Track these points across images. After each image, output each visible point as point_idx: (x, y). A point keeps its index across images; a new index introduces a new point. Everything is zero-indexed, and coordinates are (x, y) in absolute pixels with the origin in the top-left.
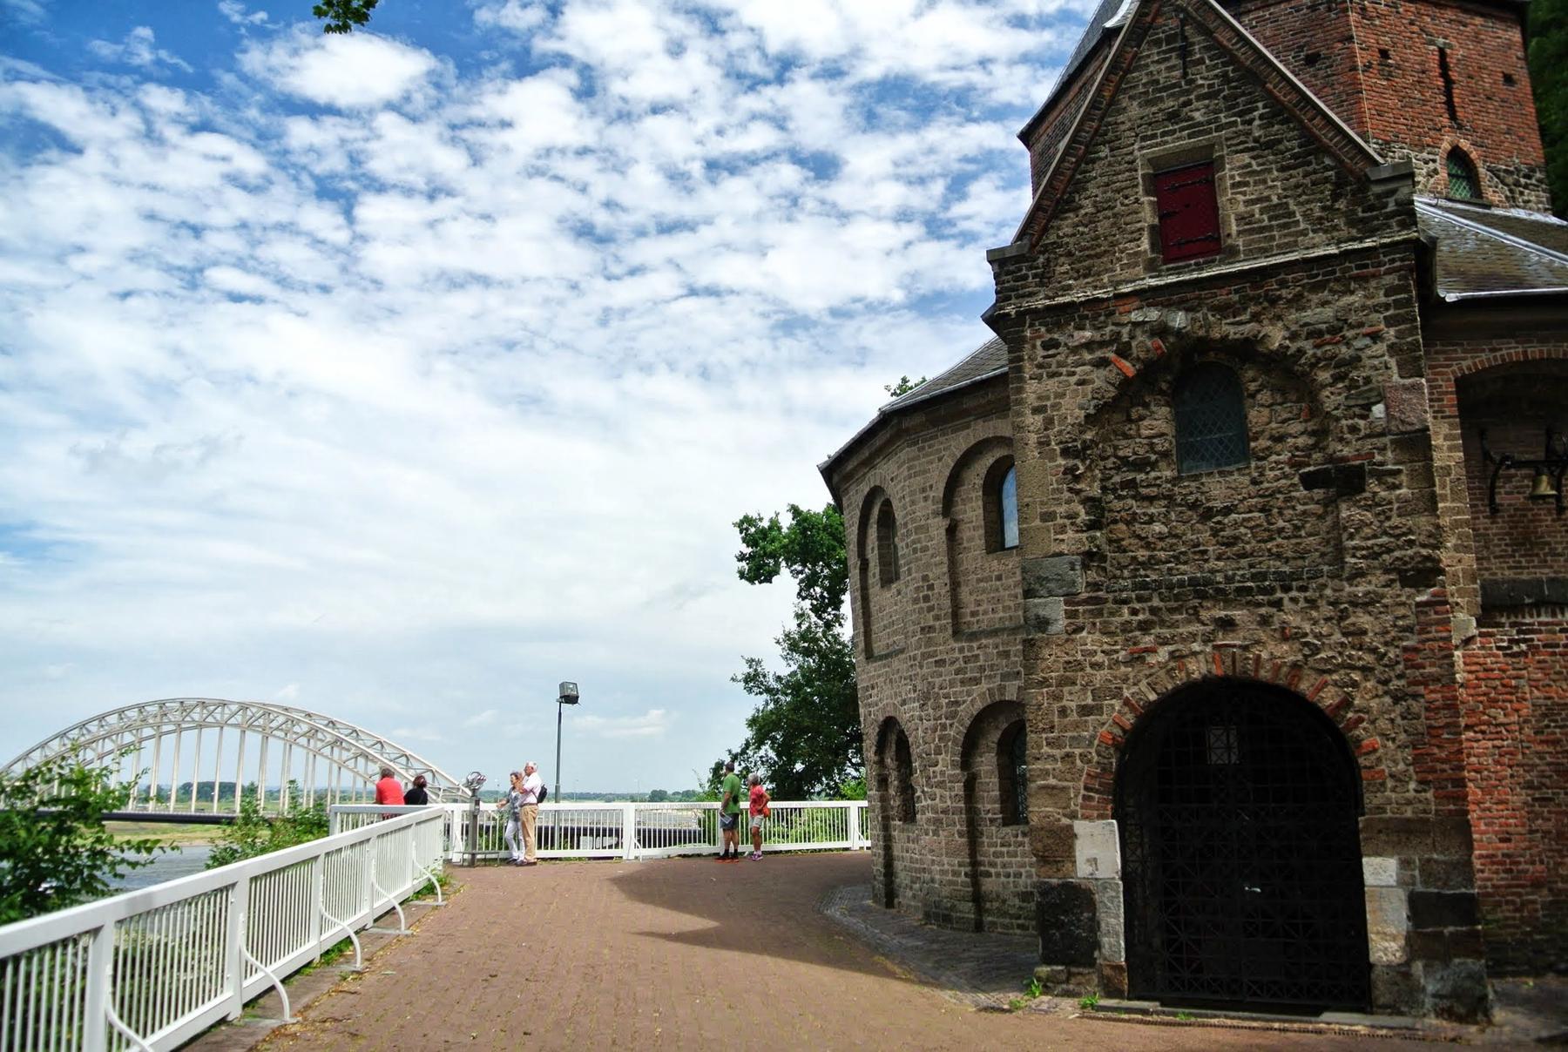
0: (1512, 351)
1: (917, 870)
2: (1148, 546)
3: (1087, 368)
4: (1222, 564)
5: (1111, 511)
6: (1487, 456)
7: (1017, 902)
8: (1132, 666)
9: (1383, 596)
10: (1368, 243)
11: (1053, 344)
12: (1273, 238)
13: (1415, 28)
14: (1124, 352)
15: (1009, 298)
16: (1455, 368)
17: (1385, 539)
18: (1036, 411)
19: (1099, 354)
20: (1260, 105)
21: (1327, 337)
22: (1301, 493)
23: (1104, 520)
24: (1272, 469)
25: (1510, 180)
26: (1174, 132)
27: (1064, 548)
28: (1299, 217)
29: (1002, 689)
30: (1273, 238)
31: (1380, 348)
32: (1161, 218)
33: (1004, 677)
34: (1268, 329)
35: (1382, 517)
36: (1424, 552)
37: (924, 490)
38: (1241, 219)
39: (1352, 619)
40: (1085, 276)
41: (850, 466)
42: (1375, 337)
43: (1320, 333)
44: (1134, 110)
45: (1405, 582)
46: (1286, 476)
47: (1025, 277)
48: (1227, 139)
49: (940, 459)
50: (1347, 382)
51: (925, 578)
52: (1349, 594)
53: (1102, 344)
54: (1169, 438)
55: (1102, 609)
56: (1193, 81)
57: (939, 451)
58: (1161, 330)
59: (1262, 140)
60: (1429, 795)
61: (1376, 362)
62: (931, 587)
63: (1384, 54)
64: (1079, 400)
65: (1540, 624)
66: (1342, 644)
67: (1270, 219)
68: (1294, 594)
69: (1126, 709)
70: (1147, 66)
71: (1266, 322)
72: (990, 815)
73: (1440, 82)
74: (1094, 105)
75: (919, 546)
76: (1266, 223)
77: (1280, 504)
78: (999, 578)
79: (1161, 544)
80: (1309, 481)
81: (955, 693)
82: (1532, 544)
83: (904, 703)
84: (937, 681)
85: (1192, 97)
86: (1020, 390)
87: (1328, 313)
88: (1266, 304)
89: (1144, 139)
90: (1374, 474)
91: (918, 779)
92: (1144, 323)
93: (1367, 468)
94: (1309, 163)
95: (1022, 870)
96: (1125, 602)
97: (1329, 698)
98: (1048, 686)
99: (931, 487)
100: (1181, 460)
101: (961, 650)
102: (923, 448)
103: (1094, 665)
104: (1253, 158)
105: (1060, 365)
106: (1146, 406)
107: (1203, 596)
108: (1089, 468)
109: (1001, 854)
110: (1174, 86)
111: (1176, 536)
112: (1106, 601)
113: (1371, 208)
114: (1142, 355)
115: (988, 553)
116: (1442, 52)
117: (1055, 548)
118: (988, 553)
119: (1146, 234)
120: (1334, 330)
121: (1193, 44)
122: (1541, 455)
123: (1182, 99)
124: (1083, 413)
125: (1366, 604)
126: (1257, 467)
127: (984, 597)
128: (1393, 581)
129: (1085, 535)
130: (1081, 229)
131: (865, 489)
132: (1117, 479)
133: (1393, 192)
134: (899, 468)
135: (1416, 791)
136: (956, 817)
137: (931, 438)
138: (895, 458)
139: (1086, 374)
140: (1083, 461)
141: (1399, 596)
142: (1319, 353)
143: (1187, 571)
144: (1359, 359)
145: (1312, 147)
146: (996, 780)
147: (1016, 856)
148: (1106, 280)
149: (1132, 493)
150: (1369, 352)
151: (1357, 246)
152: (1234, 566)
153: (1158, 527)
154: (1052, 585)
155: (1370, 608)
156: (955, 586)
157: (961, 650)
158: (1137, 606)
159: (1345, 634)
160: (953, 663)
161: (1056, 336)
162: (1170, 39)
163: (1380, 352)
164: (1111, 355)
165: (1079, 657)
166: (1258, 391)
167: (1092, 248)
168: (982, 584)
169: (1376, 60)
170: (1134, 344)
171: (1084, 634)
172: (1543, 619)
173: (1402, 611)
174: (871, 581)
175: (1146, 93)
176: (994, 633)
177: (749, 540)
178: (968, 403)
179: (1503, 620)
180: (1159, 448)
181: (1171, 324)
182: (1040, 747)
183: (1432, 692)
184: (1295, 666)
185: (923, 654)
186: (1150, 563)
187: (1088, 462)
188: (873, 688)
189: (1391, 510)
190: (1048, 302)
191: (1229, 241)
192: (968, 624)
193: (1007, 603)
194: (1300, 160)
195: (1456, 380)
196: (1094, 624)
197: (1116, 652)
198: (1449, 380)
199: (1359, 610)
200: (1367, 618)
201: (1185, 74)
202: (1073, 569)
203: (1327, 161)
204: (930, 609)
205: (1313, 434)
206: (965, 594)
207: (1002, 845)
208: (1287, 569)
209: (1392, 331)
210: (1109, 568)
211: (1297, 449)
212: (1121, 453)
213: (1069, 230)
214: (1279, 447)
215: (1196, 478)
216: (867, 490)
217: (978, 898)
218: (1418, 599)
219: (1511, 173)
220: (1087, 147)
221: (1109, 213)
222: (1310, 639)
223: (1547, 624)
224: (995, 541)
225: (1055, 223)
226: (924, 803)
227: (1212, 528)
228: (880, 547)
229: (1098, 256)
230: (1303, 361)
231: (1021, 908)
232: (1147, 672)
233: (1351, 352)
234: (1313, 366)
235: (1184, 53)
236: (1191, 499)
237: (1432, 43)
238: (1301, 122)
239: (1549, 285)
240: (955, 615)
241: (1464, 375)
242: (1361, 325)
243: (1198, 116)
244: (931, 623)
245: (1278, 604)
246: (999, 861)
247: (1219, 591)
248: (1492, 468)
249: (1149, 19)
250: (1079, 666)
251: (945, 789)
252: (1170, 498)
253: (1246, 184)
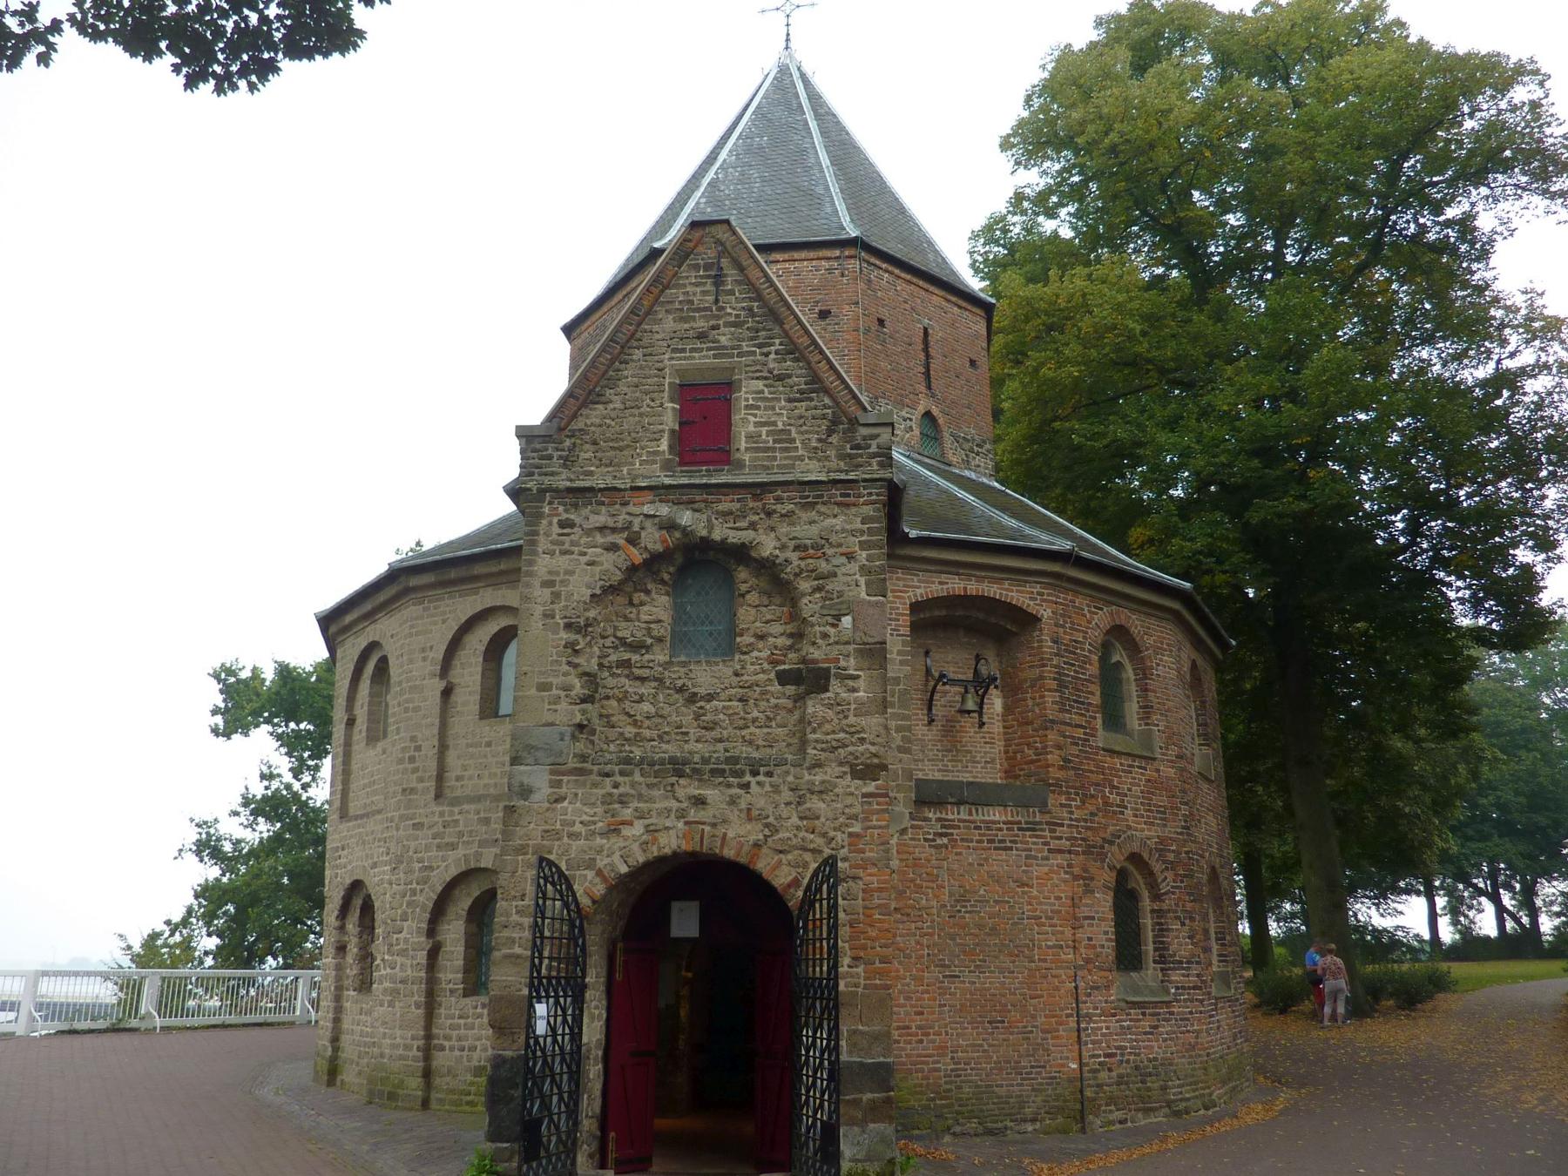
0: (955, 585)
1: (365, 1044)
2: (635, 723)
3: (598, 550)
4: (700, 746)
5: (605, 687)
6: (928, 672)
7: (469, 1078)
8: (608, 839)
9: (835, 786)
10: (851, 476)
11: (571, 525)
12: (775, 458)
14: (633, 541)
15: (532, 474)
16: (911, 594)
17: (842, 735)
18: (548, 584)
19: (611, 538)
20: (777, 341)
21: (811, 551)
22: (776, 688)
23: (597, 696)
24: (752, 664)
25: (967, 446)
26: (701, 350)
27: (558, 718)
28: (798, 444)
29: (478, 856)
30: (775, 458)
31: (853, 567)
32: (681, 424)
33: (482, 844)
34: (762, 538)
35: (841, 716)
36: (873, 749)
37: (423, 650)
38: (749, 437)
39: (808, 805)
40: (606, 466)
41: (348, 619)
42: (850, 557)
43: (805, 548)
44: (669, 323)
45: (857, 774)
46: (764, 672)
47: (550, 457)
48: (747, 366)
49: (444, 621)
50: (823, 594)
51: (413, 739)
52: (808, 782)
53: (614, 530)
54: (665, 624)
55: (585, 781)
56: (723, 308)
57: (444, 613)
58: (670, 526)
59: (775, 372)
60: (860, 969)
61: (849, 578)
62: (418, 748)
63: (881, 322)
64: (587, 579)
65: (959, 820)
66: (798, 828)
67: (775, 441)
68: (761, 778)
69: (598, 880)
70: (684, 286)
71: (761, 531)
72: (451, 986)
73: (922, 356)
74: (633, 311)
75: (411, 705)
76: (771, 444)
77: (756, 696)
78: (489, 744)
79: (647, 723)
80: (783, 678)
81: (429, 858)
82: (957, 751)
83: (375, 865)
84: (413, 844)
85: (721, 322)
86: (531, 563)
87: (814, 530)
88: (762, 516)
89: (675, 350)
90: (837, 676)
91: (379, 947)
92: (654, 516)
93: (833, 671)
94: (811, 400)
95: (478, 1043)
96: (607, 775)
98: (524, 854)
99: (431, 648)
100: (673, 646)
101: (442, 814)
102: (429, 608)
103: (570, 835)
104: (766, 386)
105: (573, 543)
106: (648, 592)
107: (680, 774)
108: (589, 644)
109: (458, 1027)
110: (705, 309)
111: (661, 716)
112: (590, 772)
113: (857, 447)
114: (650, 546)
115: (481, 719)
116: (926, 330)
117: (549, 718)
118: (481, 719)
119: (666, 435)
120: (816, 547)
121: (726, 275)
122: (970, 676)
123: (711, 323)
124: (589, 592)
125: (821, 792)
126: (740, 661)
127: (471, 762)
128: (845, 773)
129: (578, 707)
130: (608, 421)
131: (362, 643)
132: (613, 658)
133: (877, 436)
134: (401, 625)
135: (849, 966)
136: (415, 987)
137: (437, 600)
138: (398, 616)
139: (597, 556)
140: (585, 636)
141: (849, 786)
142: (803, 564)
143: (671, 749)
144: (835, 575)
145: (816, 384)
146: (462, 949)
147: (473, 1029)
148: (625, 472)
149: (626, 672)
150: (843, 570)
151: (843, 476)
152: (711, 748)
153: (646, 707)
154: (539, 754)
155: (824, 796)
156: (443, 748)
157: (442, 814)
158: (619, 779)
159: (801, 818)
160: (430, 827)
161: (572, 517)
162: (707, 267)
163: (852, 572)
164: (622, 542)
165: (558, 826)
166: (749, 592)
167: (616, 440)
168: (471, 750)
169: (875, 326)
170: (643, 534)
171: (565, 804)
172: (963, 816)
173: (849, 800)
174: (356, 737)
175: (682, 310)
176: (478, 799)
177: (227, 691)
178: (479, 569)
179: (931, 815)
180: (655, 633)
181: (678, 521)
182: (508, 915)
183: (870, 875)
184: (757, 845)
185: (401, 817)
186: (637, 739)
187: (589, 638)
188: (343, 849)
189: (849, 710)
190: (568, 484)
191: (738, 455)
192: (452, 788)
193: (493, 770)
194: (804, 396)
195: (911, 605)
196: (576, 795)
197: (594, 823)
198: (905, 604)
199: (814, 797)
200: (823, 805)
201: (717, 301)
202: (562, 740)
203: (827, 401)
204: (416, 770)
205: (791, 635)
206: (452, 758)
207: (460, 1017)
208: (756, 755)
209: (864, 554)
210: (597, 741)
211: (776, 648)
212: (619, 634)
213: (598, 421)
214: (761, 645)
215: (684, 664)
216: (364, 644)
217: (427, 1074)
218: (864, 790)
219: (968, 441)
220: (622, 347)
221: (636, 412)
222: (771, 820)
223: (965, 821)
224: (489, 707)
225: (584, 411)
226: (383, 972)
227: (695, 712)
228: (370, 704)
229: (621, 449)
230: (788, 570)
231: (472, 1084)
232: (622, 845)
233: (829, 567)
234: (796, 575)
235: (718, 280)
236: (679, 683)
237: (919, 321)
238: (809, 363)
239: (987, 535)
240: (440, 778)
241: (917, 602)
242: (840, 545)
243: (724, 340)
244: (414, 785)
245: (747, 786)
246: (454, 1033)
247: (695, 771)
248: (932, 683)
249: (691, 245)
250: (557, 835)
251: (407, 956)
252: (660, 680)
253: (758, 408)
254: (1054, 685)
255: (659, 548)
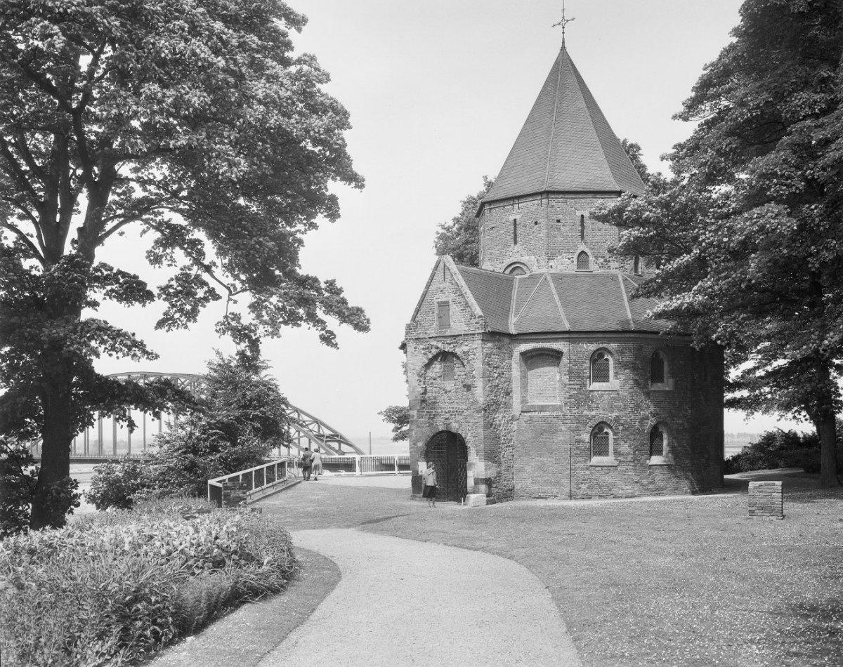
13: (573, 209)
58: (438, 348)
63: (558, 221)
97: (463, 435)
116: (582, 216)
254: (567, 373)
255: (435, 354)
